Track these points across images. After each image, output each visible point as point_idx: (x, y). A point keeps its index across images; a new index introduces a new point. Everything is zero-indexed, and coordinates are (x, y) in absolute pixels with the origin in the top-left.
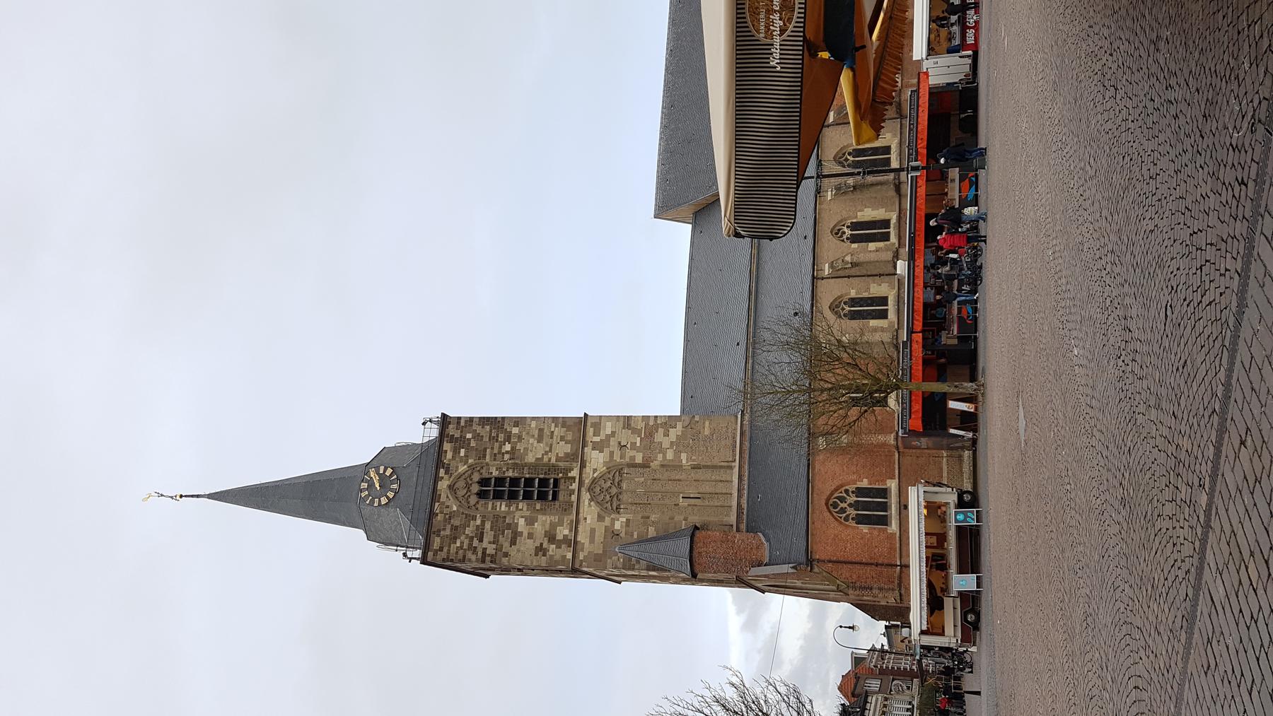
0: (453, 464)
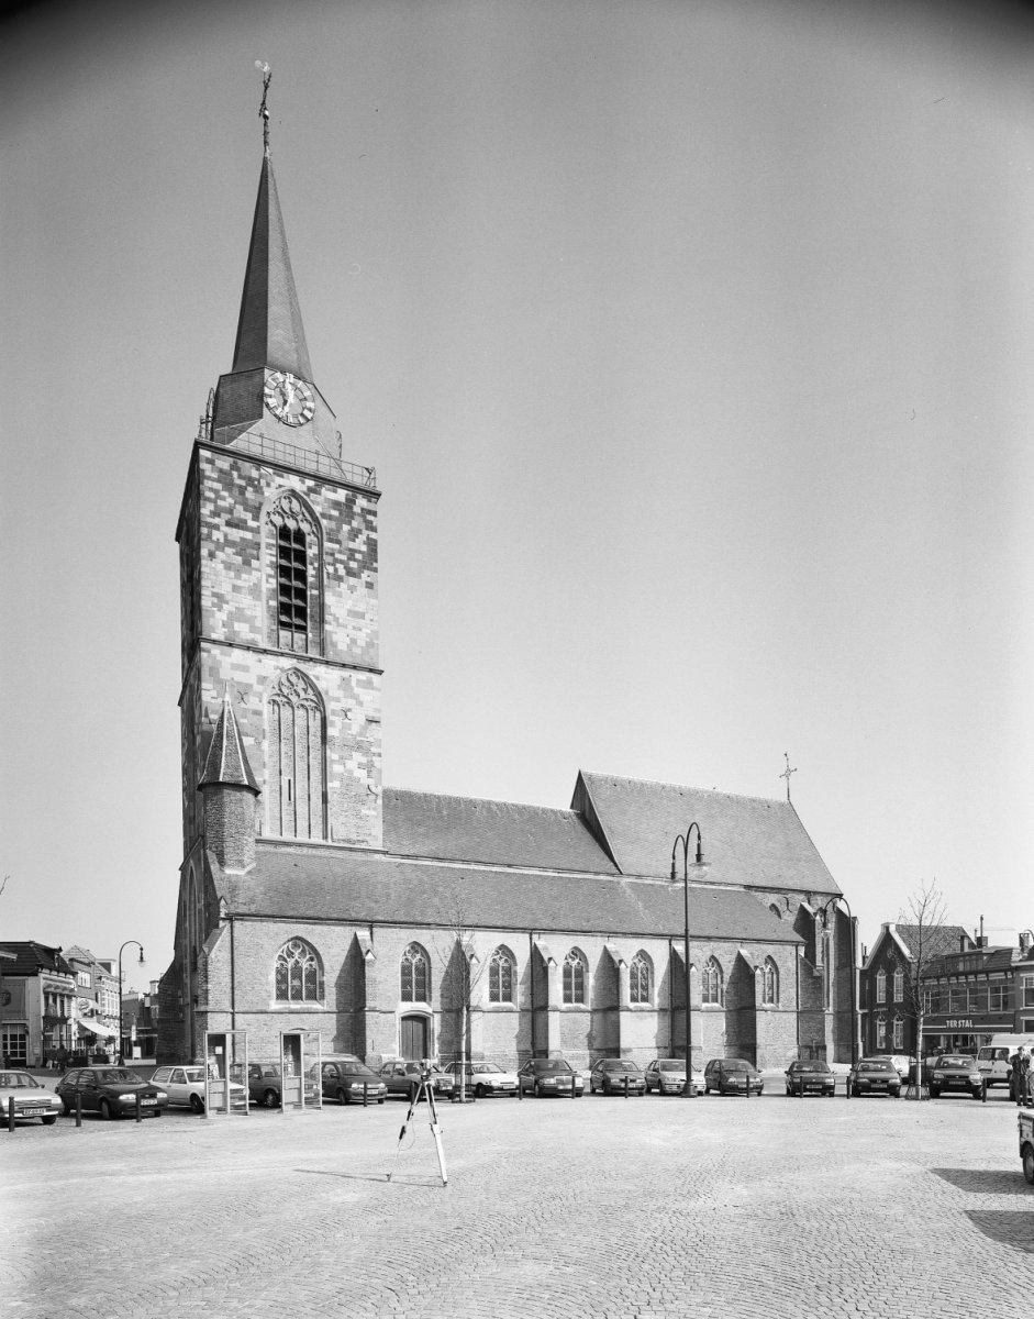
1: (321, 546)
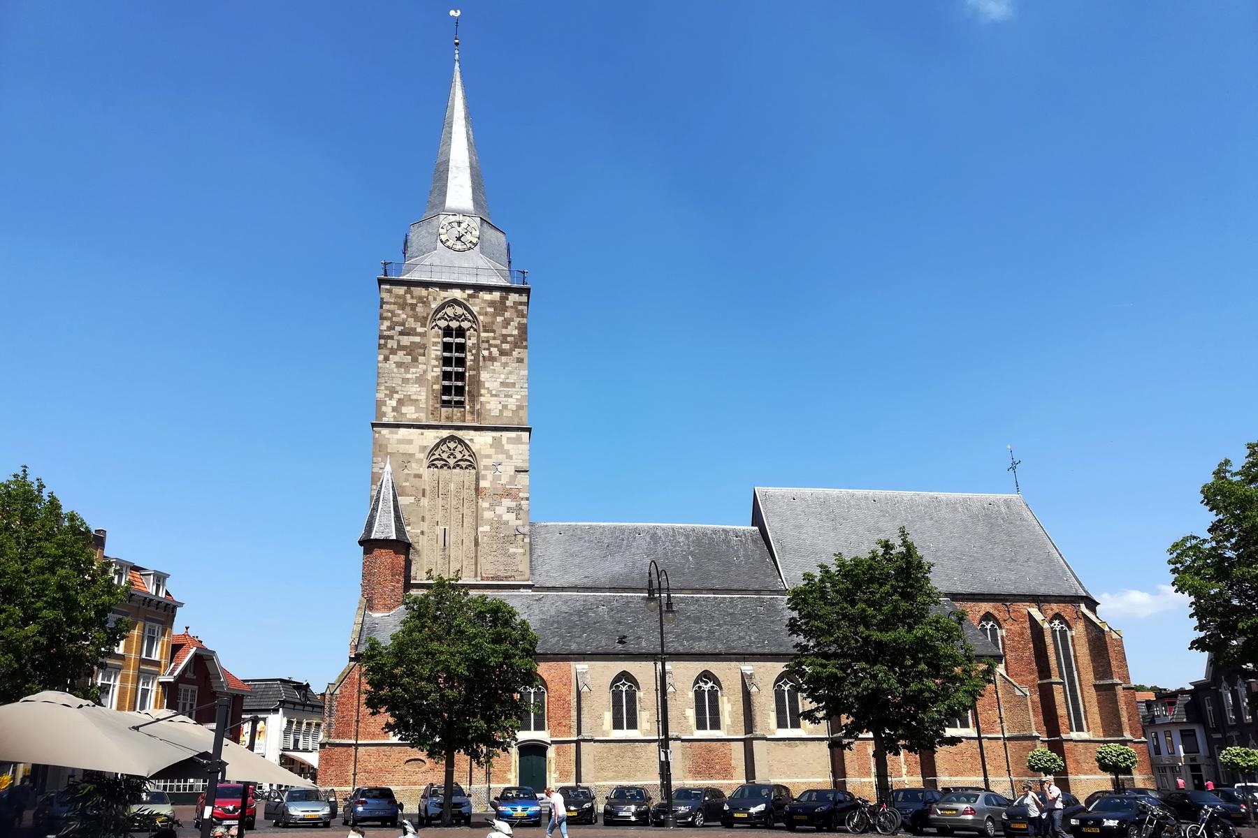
0: (477, 301)
1: (479, 336)
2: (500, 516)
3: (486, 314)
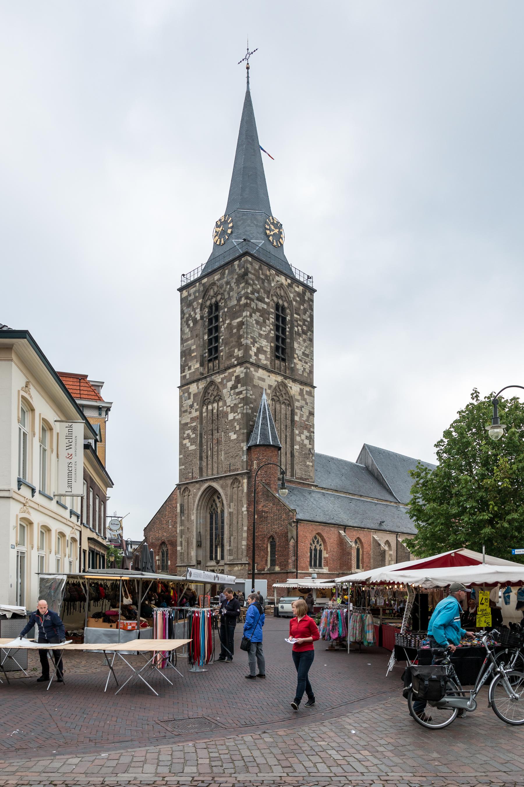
1: (292, 316)
2: (303, 441)
3: (296, 301)
